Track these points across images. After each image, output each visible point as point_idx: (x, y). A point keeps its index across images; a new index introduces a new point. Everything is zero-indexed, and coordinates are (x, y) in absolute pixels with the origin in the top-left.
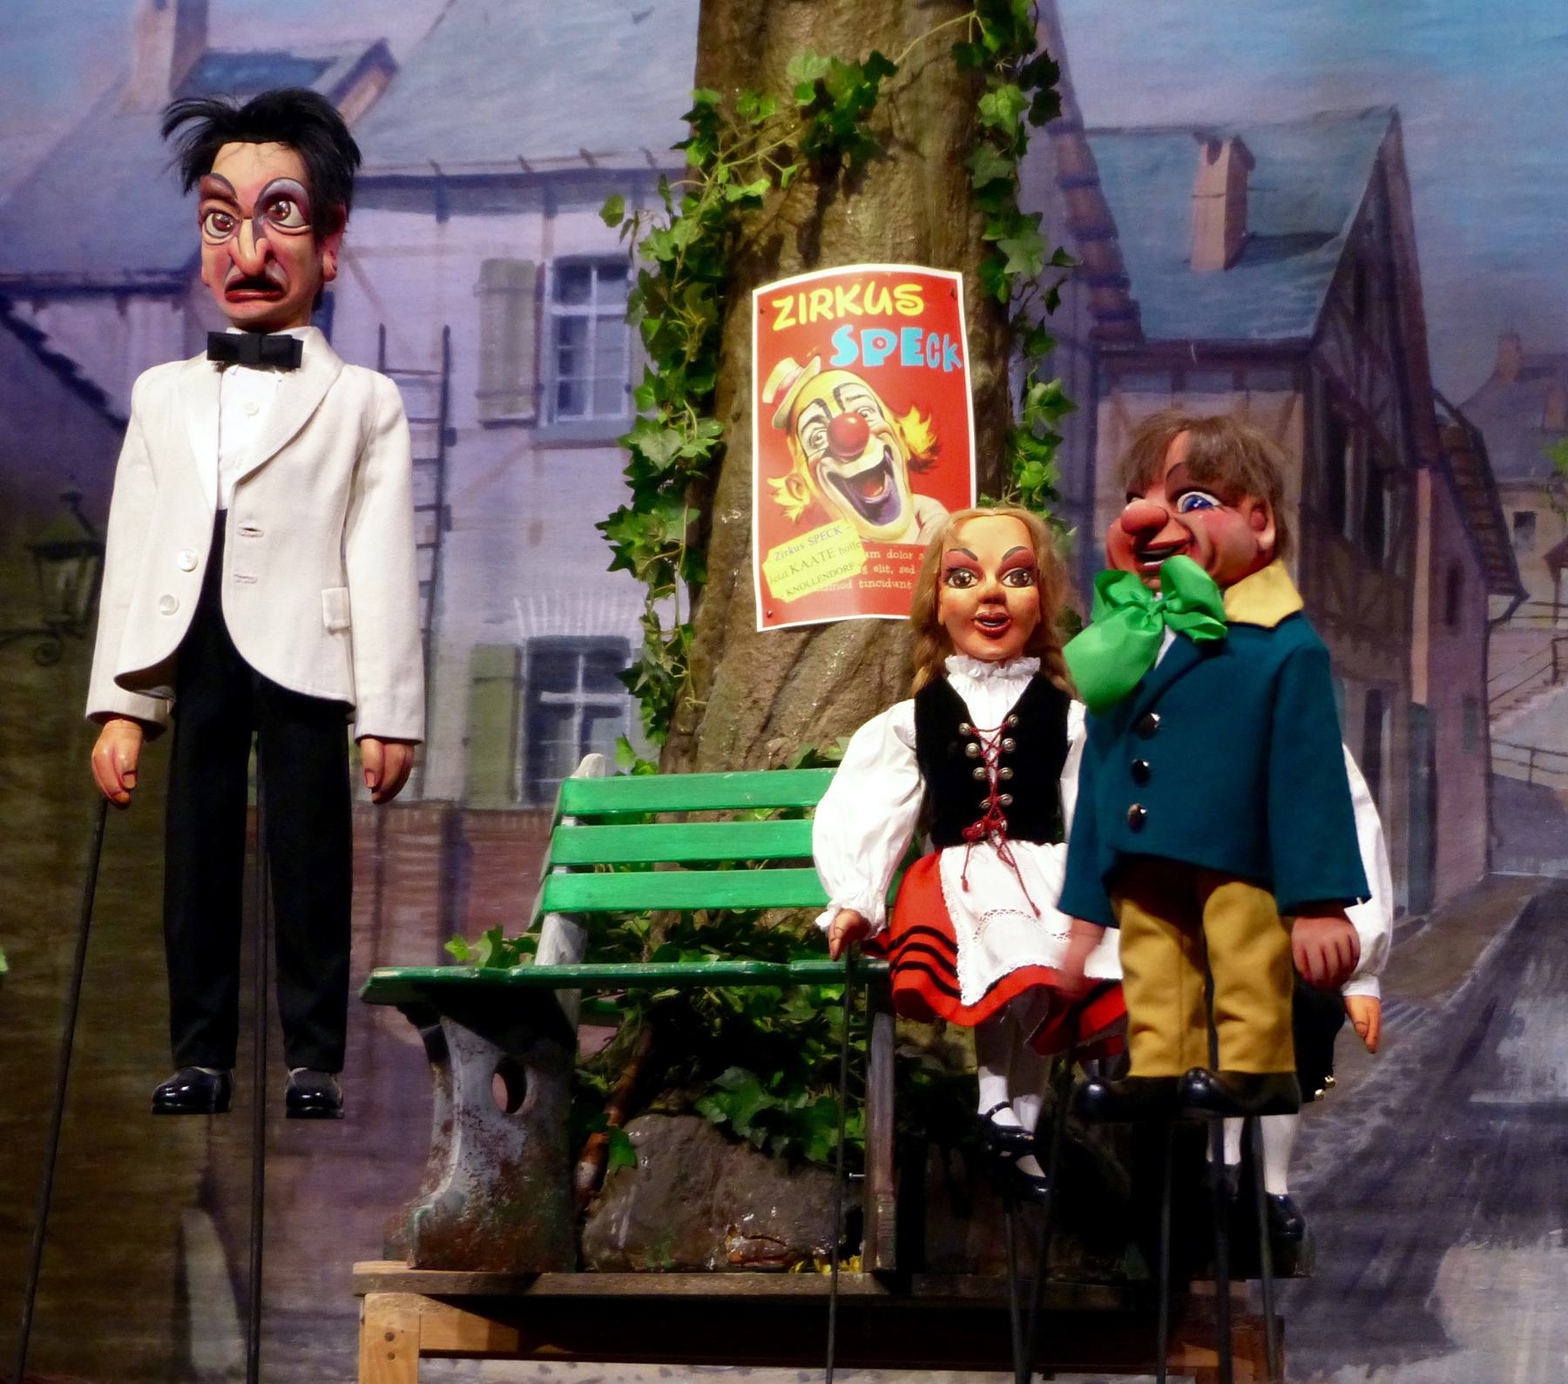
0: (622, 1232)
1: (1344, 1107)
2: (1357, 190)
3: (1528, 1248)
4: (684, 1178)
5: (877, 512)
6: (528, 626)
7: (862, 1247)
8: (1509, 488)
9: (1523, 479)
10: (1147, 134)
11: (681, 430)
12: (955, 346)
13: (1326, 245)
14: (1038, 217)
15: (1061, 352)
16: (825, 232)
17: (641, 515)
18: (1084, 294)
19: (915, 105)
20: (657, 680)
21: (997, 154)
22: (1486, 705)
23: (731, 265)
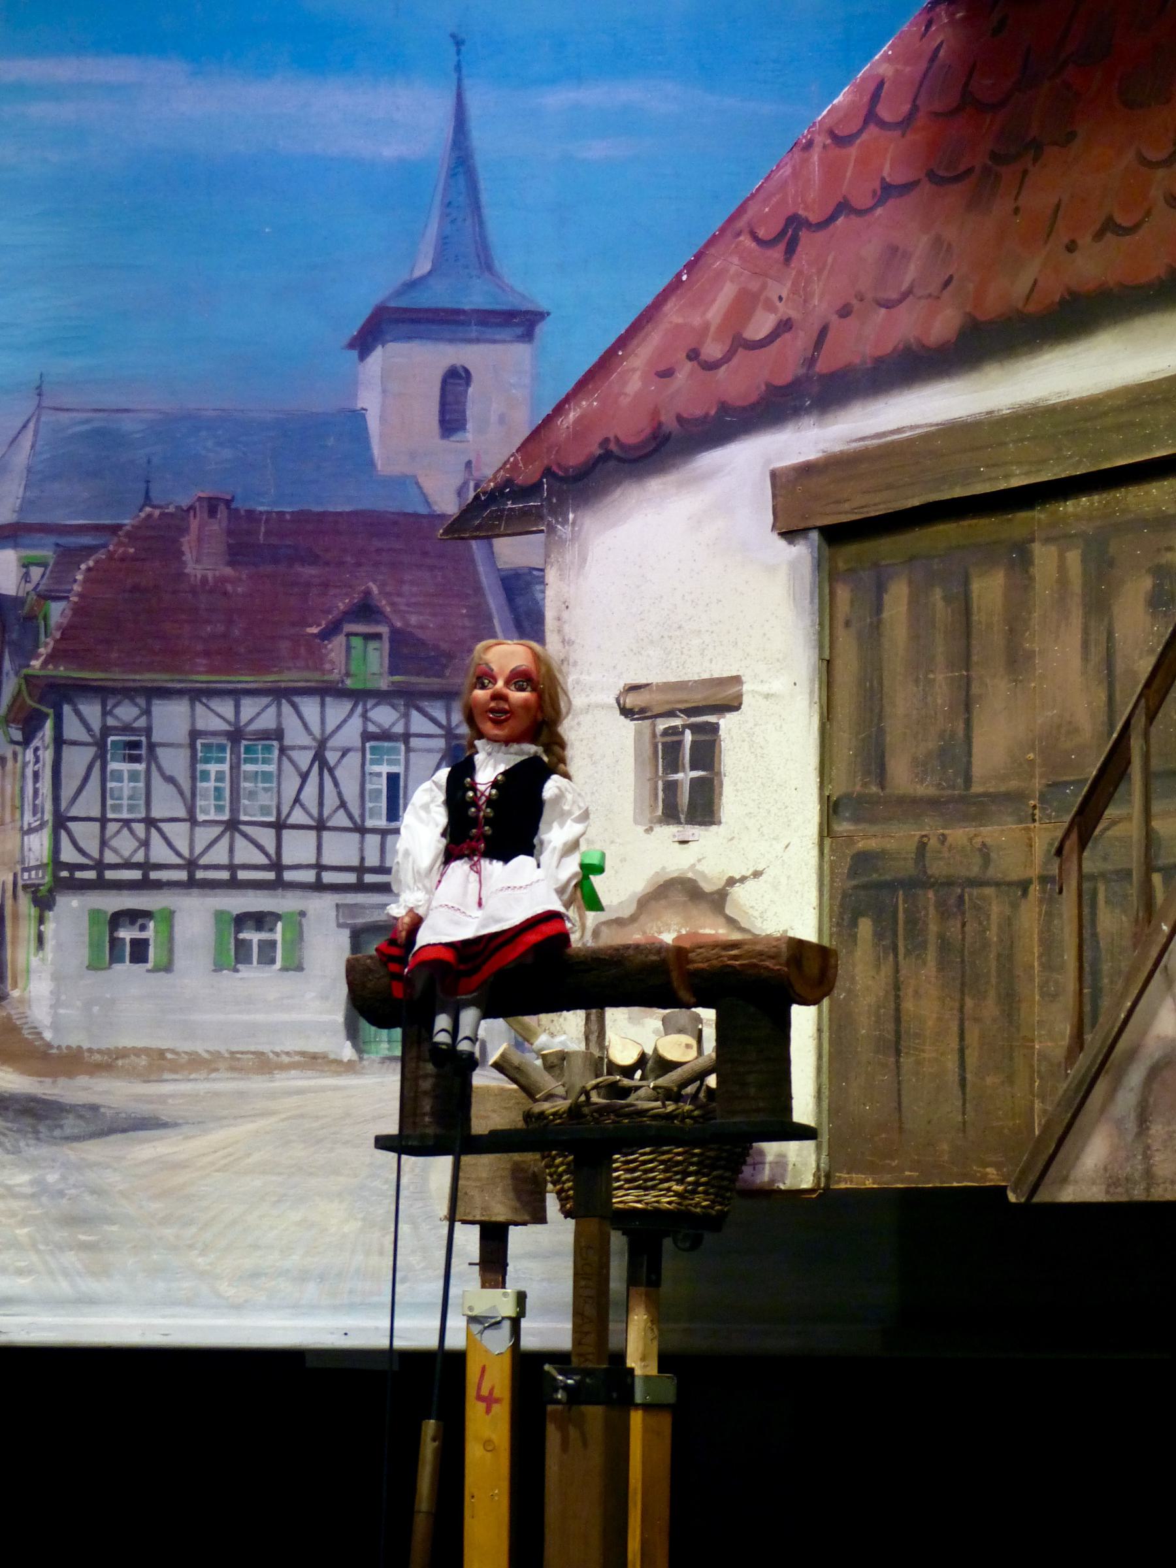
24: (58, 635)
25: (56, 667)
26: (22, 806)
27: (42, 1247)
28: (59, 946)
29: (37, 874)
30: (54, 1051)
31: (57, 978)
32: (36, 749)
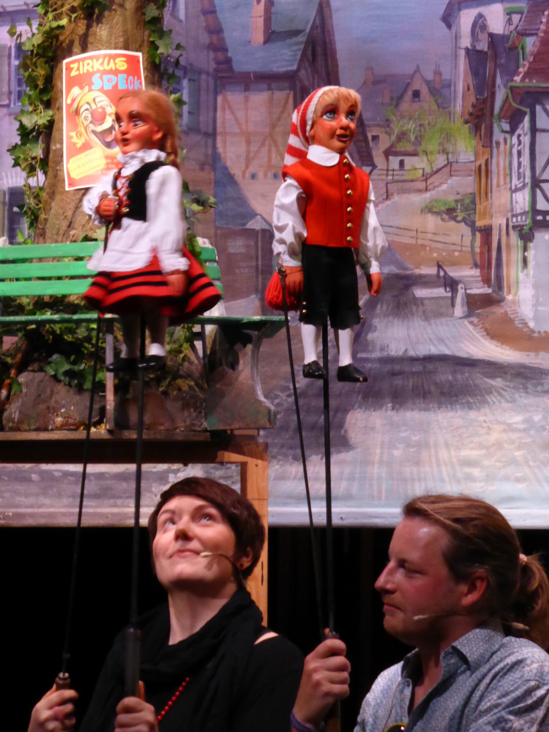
0: (16, 416)
2: (312, 14)
3: (379, 411)
4: (39, 396)
6: (8, 182)
7: (105, 421)
8: (369, 126)
9: (375, 123)
11: (37, 115)
12: (139, 81)
13: (301, 35)
14: (171, 31)
15: (204, 77)
16: (89, 38)
17: (23, 147)
18: (212, 55)
20: (30, 208)
21: (155, 7)
24: (531, 59)
25: (531, 80)
26: (511, 174)
27: (532, 464)
28: (537, 266)
29: (522, 219)
30: (536, 335)
31: (536, 286)
32: (519, 136)
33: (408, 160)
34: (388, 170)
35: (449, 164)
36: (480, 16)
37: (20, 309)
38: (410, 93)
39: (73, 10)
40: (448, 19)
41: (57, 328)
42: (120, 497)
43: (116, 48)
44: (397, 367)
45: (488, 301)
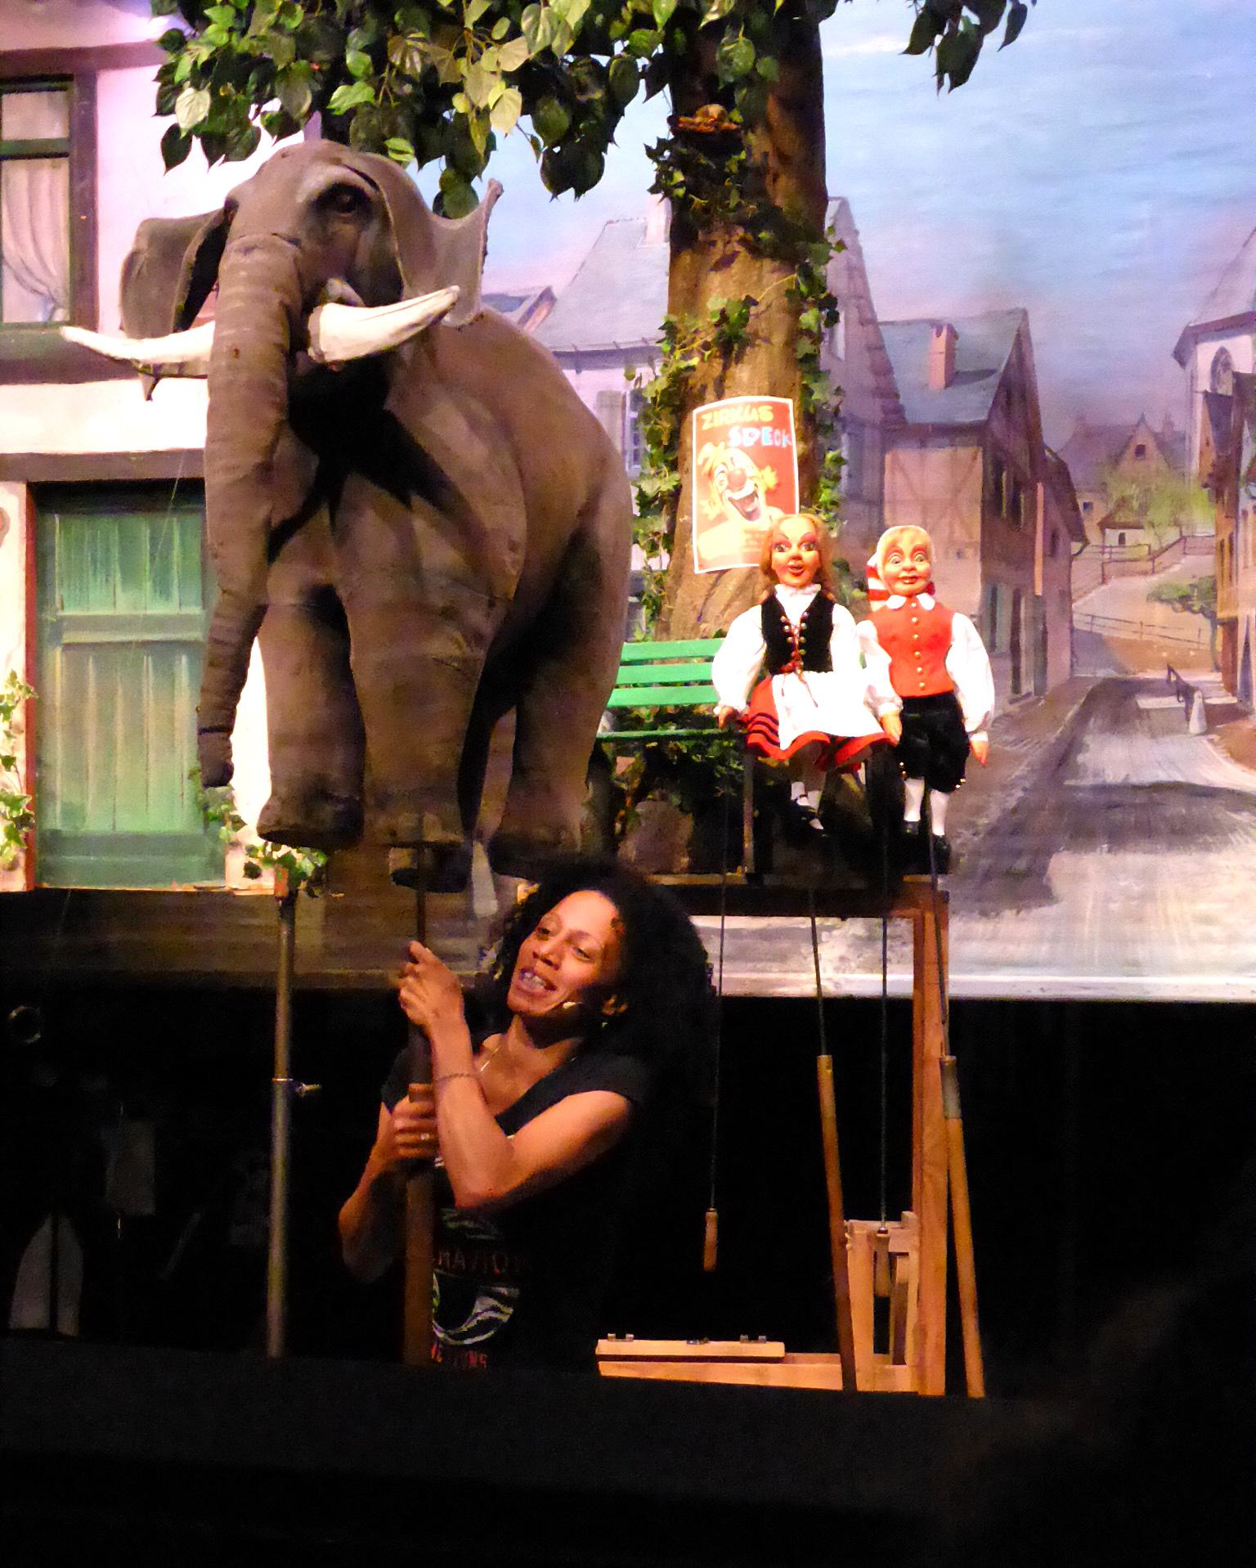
1: (1004, 787)
5: (750, 516)
10: (909, 323)
14: (829, 371)
18: (878, 402)
19: (768, 320)
22: (1070, 594)
23: (682, 401)
33: (1128, 533)
34: (1104, 547)
35: (1183, 539)
36: (1223, 351)
37: (638, 723)
38: (1132, 449)
39: (706, 346)
40: (1182, 355)
41: (683, 747)
42: (761, 960)
43: (760, 394)
44: (1116, 798)
45: (1232, 714)
